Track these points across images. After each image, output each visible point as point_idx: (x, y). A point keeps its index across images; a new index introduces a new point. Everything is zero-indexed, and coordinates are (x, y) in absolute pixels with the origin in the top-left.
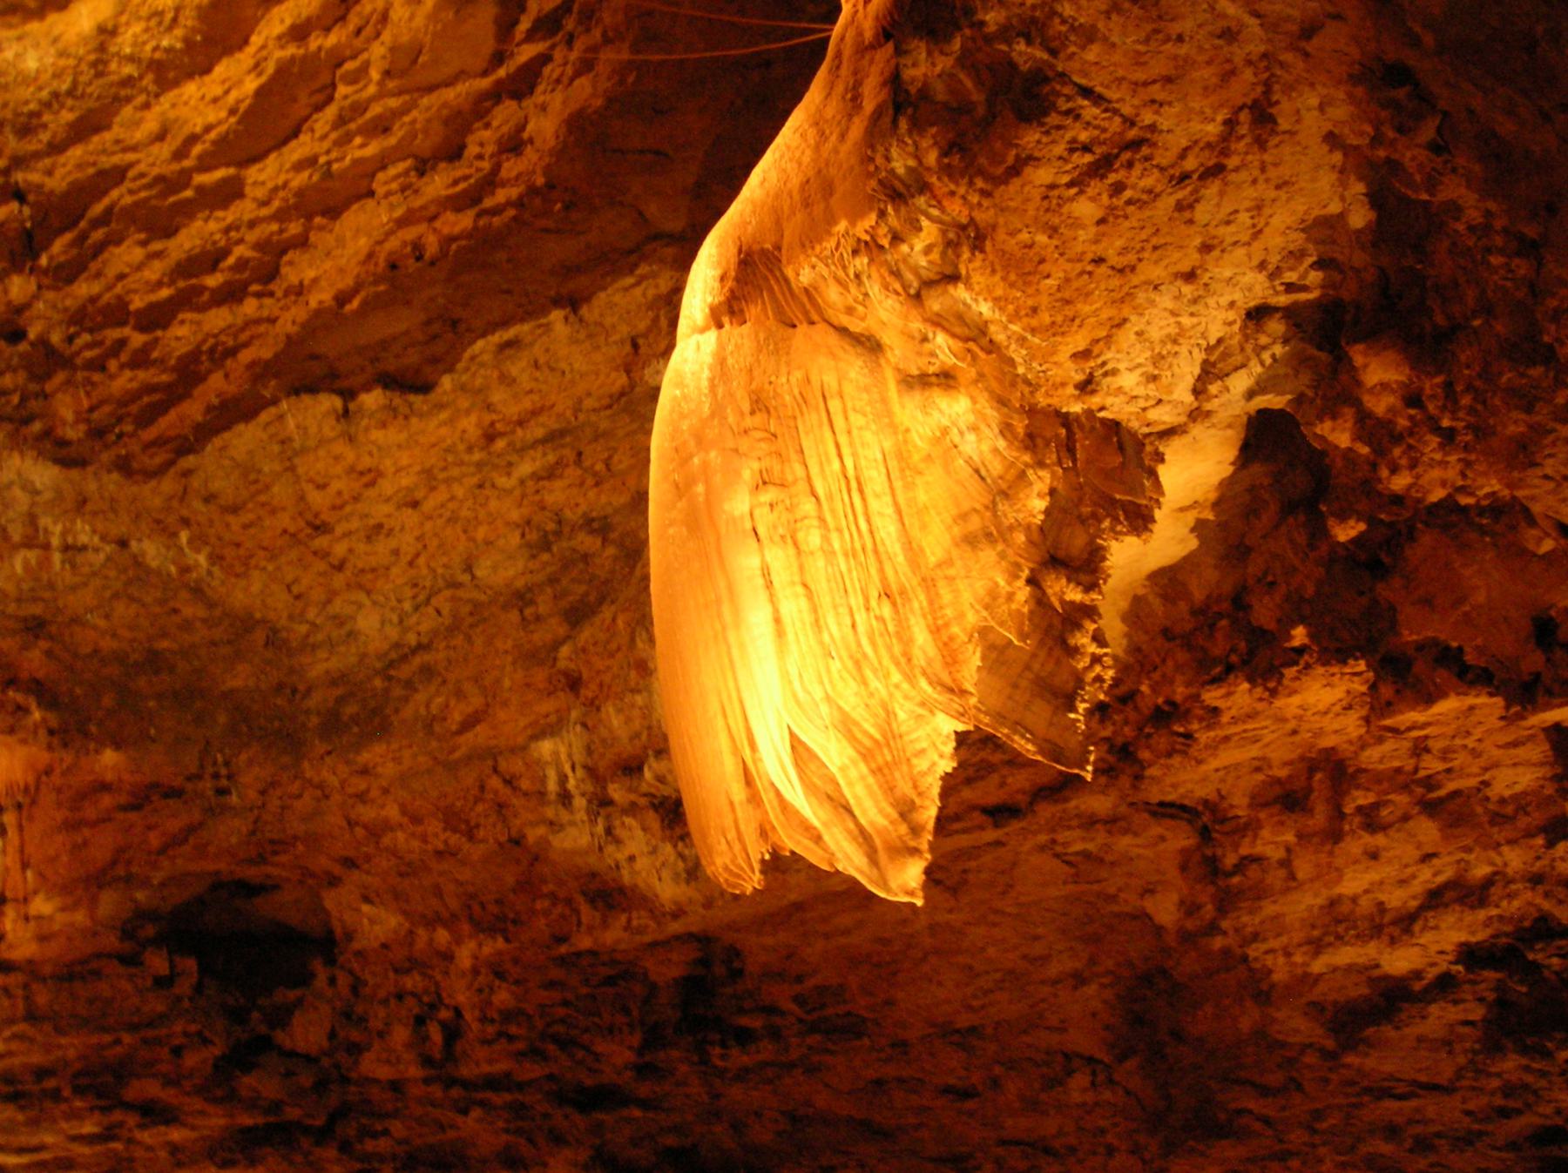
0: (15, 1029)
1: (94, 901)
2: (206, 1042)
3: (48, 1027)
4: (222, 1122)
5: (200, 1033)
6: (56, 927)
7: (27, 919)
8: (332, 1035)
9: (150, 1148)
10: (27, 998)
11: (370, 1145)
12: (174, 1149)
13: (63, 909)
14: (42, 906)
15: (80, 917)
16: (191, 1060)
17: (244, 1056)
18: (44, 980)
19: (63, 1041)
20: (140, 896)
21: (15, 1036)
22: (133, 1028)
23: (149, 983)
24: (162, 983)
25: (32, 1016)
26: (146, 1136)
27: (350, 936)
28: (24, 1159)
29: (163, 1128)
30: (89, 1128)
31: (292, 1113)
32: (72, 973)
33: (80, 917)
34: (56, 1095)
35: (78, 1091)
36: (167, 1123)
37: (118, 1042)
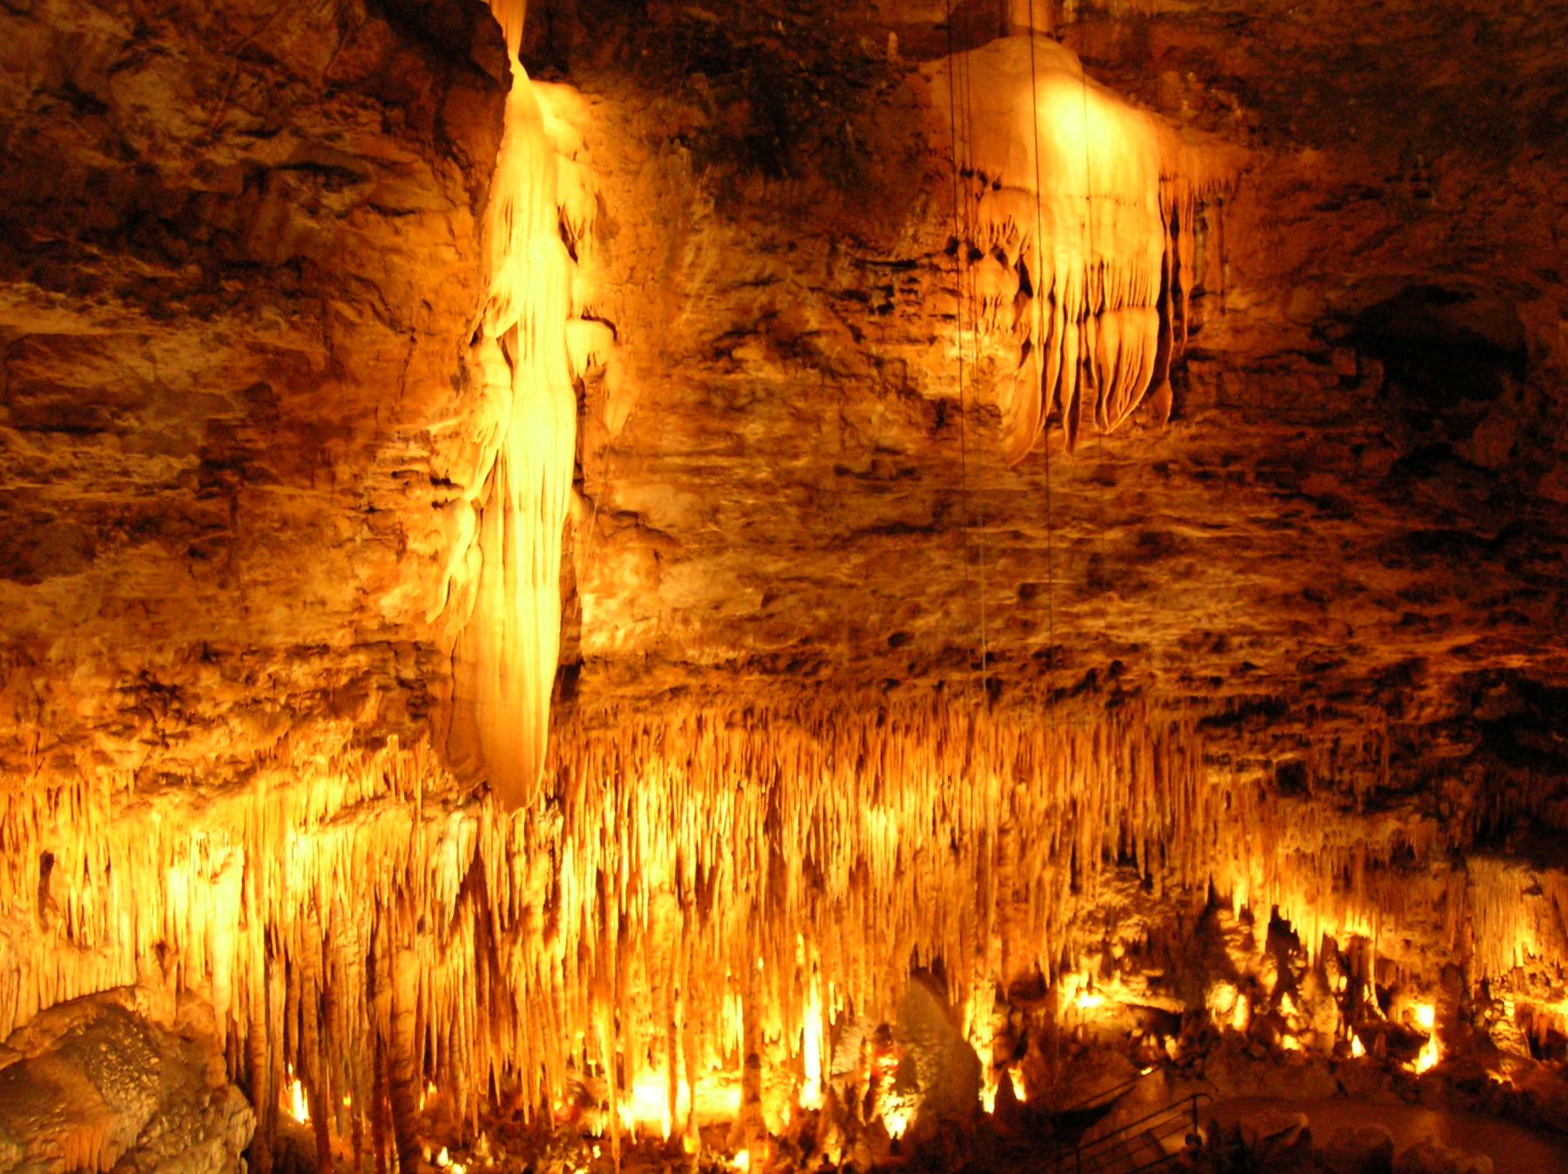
0: (1207, 414)
1: (1286, 302)
2: (1387, 444)
3: (1237, 415)
4: (1394, 523)
5: (1380, 436)
6: (1250, 322)
7: (1223, 311)
8: (1513, 452)
9: (1322, 539)
10: (1218, 387)
11: (1538, 567)
12: (1346, 543)
13: (1257, 305)
14: (1236, 300)
15: (1273, 313)
16: (1371, 459)
17: (1419, 463)
18: (1235, 370)
19: (1251, 430)
20: (1331, 295)
21: (1205, 421)
22: (1315, 423)
23: (1336, 381)
24: (1348, 383)
25: (1221, 405)
26: (1320, 528)
27: (1543, 352)
28: (1206, 535)
29: (1336, 522)
30: (1267, 513)
31: (1464, 524)
32: (1260, 368)
33: (1273, 313)
34: (1239, 479)
35: (1260, 476)
36: (1343, 517)
37: (1301, 435)
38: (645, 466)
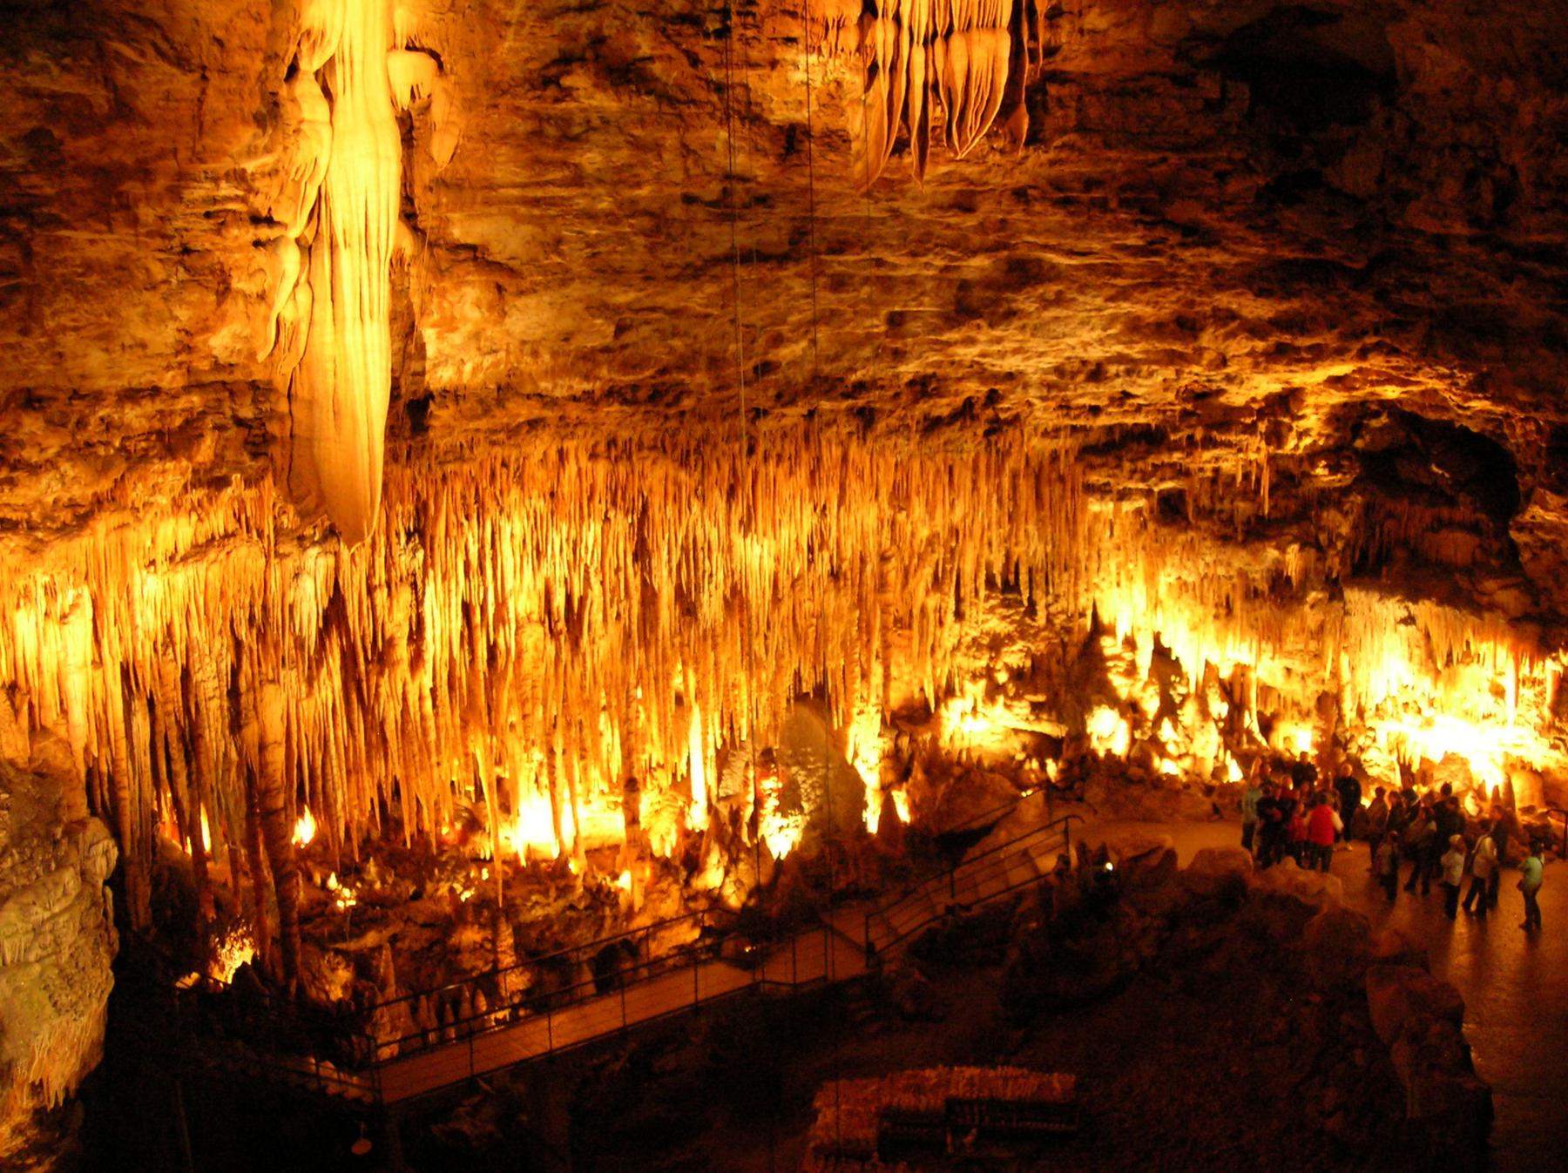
0: (1065, 138)
1: (1149, 18)
2: (1251, 170)
3: (1097, 140)
4: (1262, 251)
5: (1244, 161)
6: (1109, 43)
7: (1081, 31)
8: (1381, 180)
9: (1192, 267)
10: (1079, 110)
11: (1407, 297)
12: (1216, 271)
13: (1117, 25)
14: (1095, 20)
15: (1133, 34)
16: (1233, 187)
17: (1283, 191)
18: (1097, 93)
19: (1112, 154)
20: (1195, 15)
21: (1064, 146)
22: (1176, 149)
23: (1200, 104)
24: (1212, 106)
25: (1082, 128)
26: (1187, 255)
27: (1411, 76)
28: (1074, 262)
29: (1202, 250)
30: (1132, 240)
31: (1332, 253)
32: (1121, 91)
33: (1133, 34)
34: (1103, 205)
35: (1123, 203)
36: (1208, 245)
37: (1164, 160)
38: (479, 198)
